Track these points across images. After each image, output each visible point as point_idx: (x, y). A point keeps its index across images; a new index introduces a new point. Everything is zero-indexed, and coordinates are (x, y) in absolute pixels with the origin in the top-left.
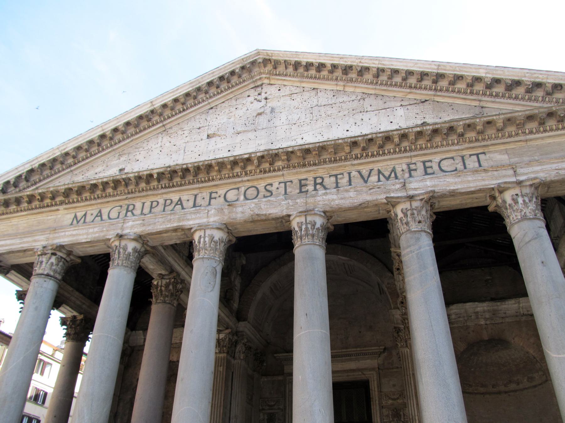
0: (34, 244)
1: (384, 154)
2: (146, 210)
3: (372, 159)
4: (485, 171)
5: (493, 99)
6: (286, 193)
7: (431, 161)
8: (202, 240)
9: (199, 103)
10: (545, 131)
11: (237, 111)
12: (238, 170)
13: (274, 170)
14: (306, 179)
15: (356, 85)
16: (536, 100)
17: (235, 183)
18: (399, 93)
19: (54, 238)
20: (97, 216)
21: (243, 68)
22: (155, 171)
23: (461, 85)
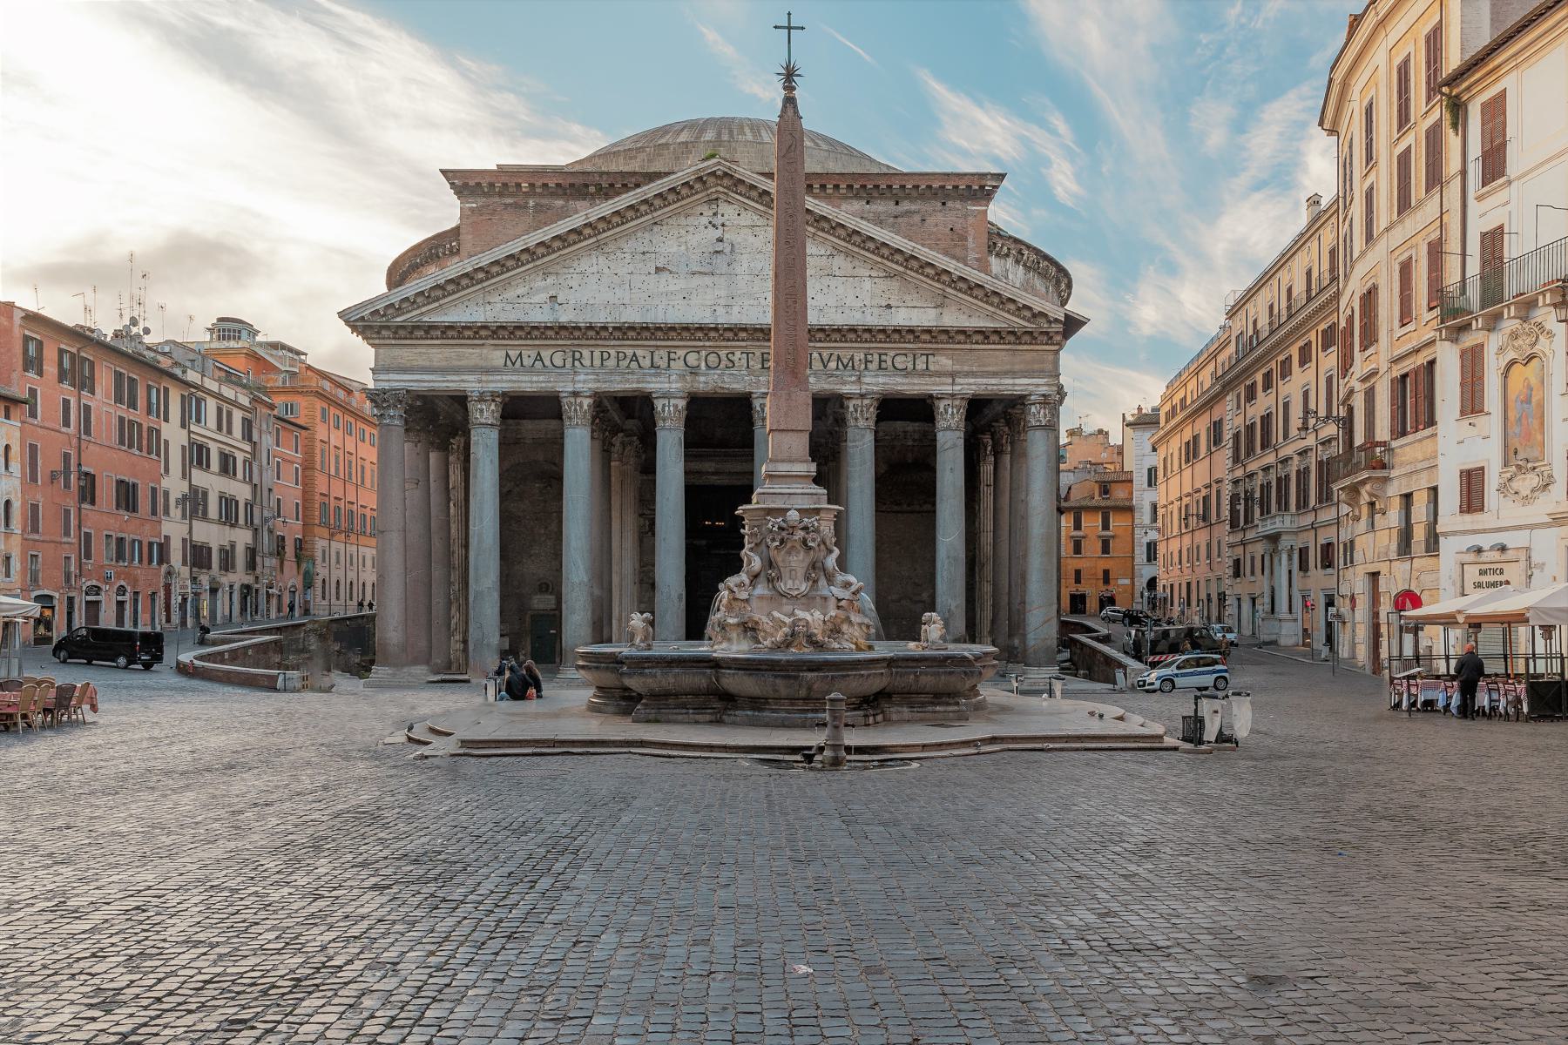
0: (463, 385)
1: (846, 341)
2: (597, 362)
5: (954, 292)
6: (748, 367)
8: (667, 408)
9: (642, 216)
10: (989, 343)
11: (690, 237)
12: (700, 334)
13: (738, 340)
16: (992, 304)
19: (487, 382)
20: (536, 360)
21: (700, 179)
23: (929, 271)
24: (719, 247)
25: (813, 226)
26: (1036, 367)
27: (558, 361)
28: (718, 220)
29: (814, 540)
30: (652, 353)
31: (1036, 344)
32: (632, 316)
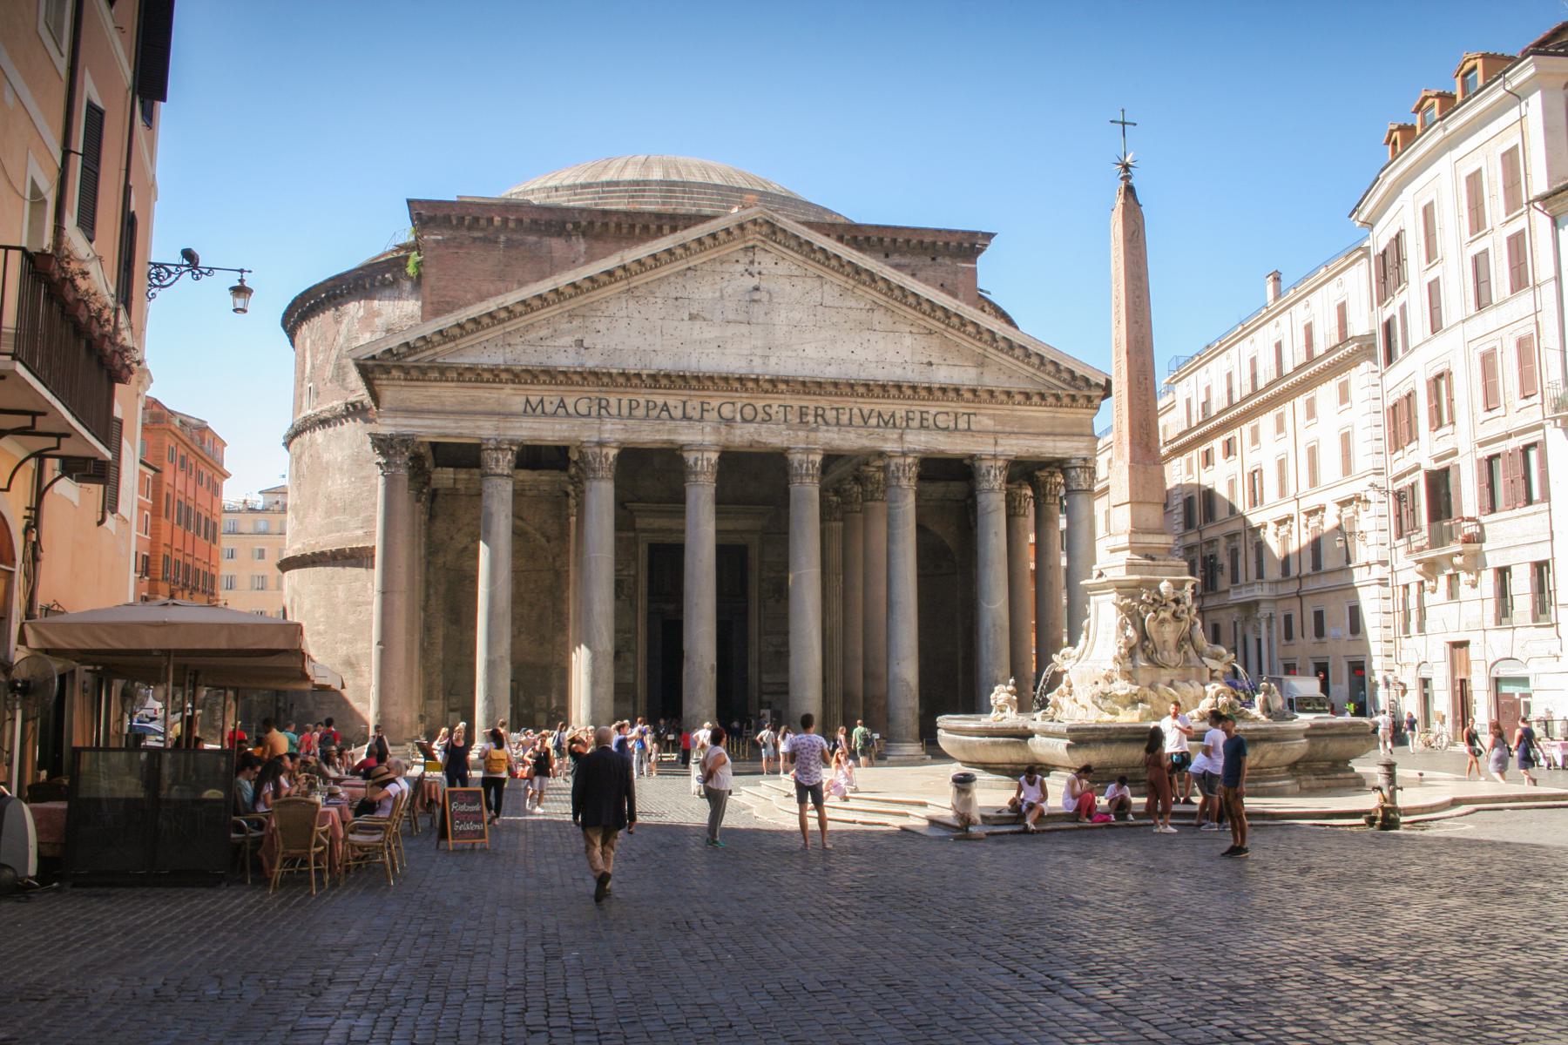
0: (478, 432)
1: (889, 397)
2: (625, 411)
3: (876, 400)
4: (973, 436)
6: (786, 421)
7: (927, 412)
8: (700, 462)
10: (1030, 405)
11: (725, 284)
13: (777, 393)
14: (807, 407)
15: (868, 290)
16: (1033, 366)
17: (732, 397)
18: (912, 314)
20: (559, 407)
22: (645, 372)
24: (757, 296)
25: (853, 278)
26: (1076, 430)
27: (583, 409)
28: (755, 268)
29: (1183, 612)
30: (684, 403)
31: (1076, 407)
32: (664, 363)
